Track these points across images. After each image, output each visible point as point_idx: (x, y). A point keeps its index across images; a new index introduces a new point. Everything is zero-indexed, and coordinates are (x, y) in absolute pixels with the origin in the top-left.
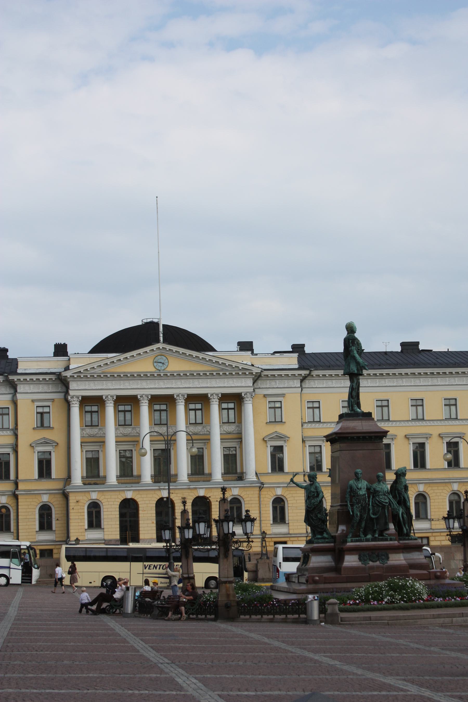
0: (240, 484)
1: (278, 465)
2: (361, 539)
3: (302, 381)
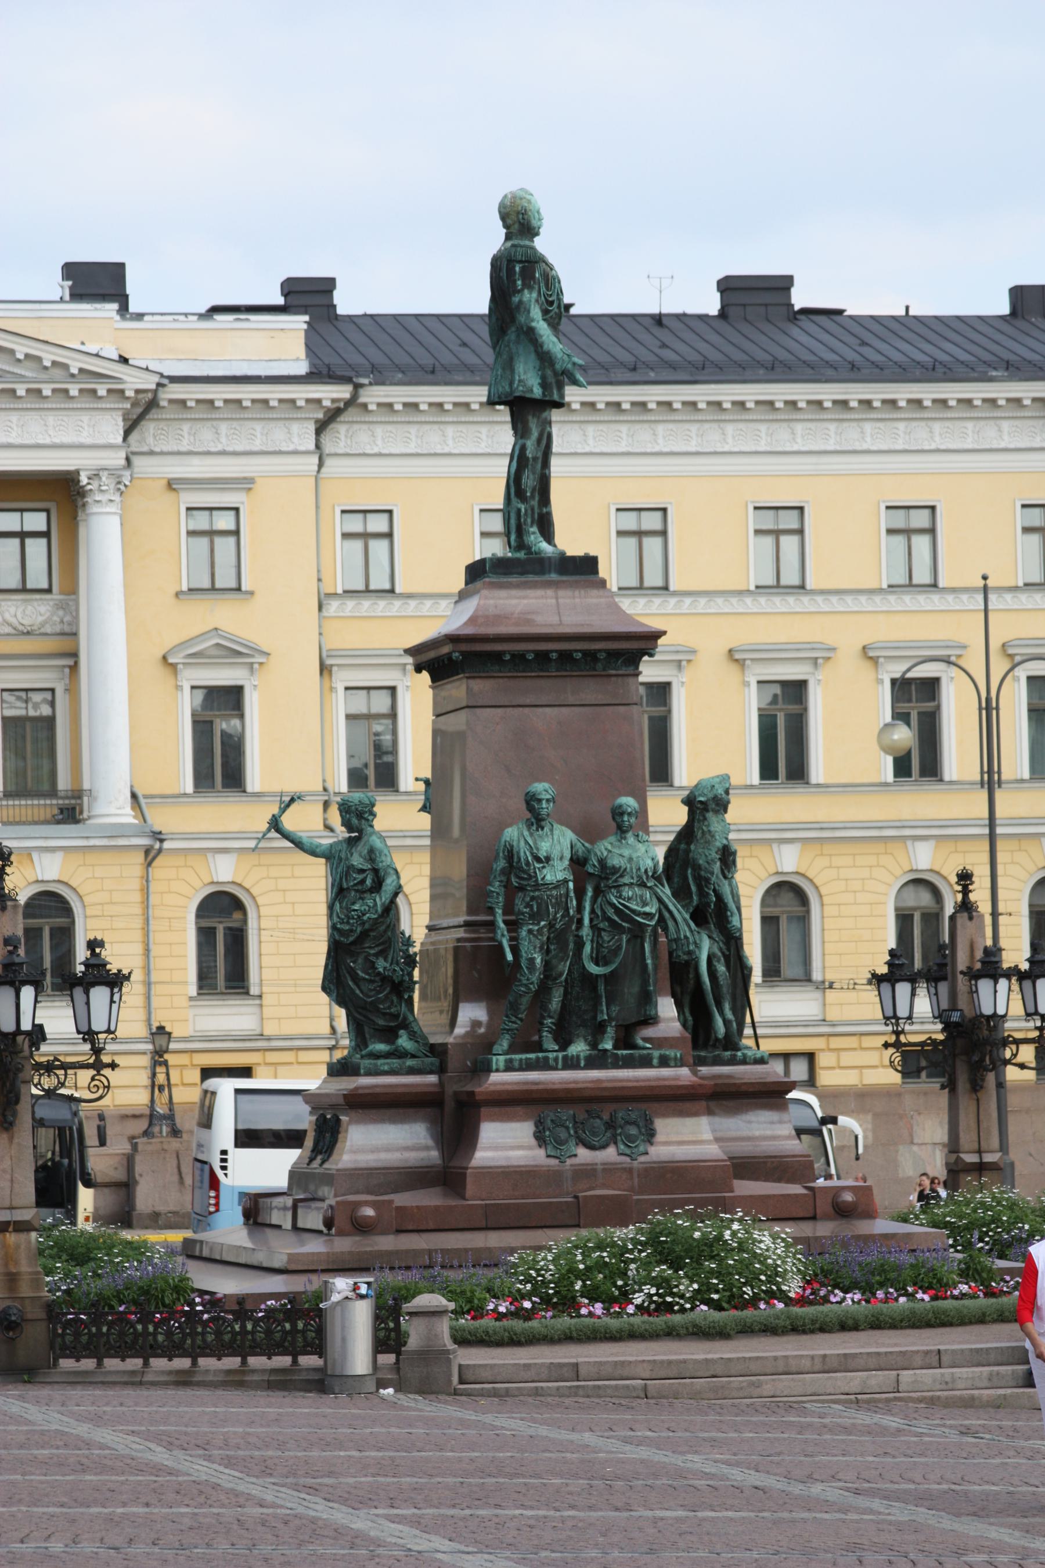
0: (67, 835)
1: (220, 764)
2: (546, 1059)
3: (321, 428)
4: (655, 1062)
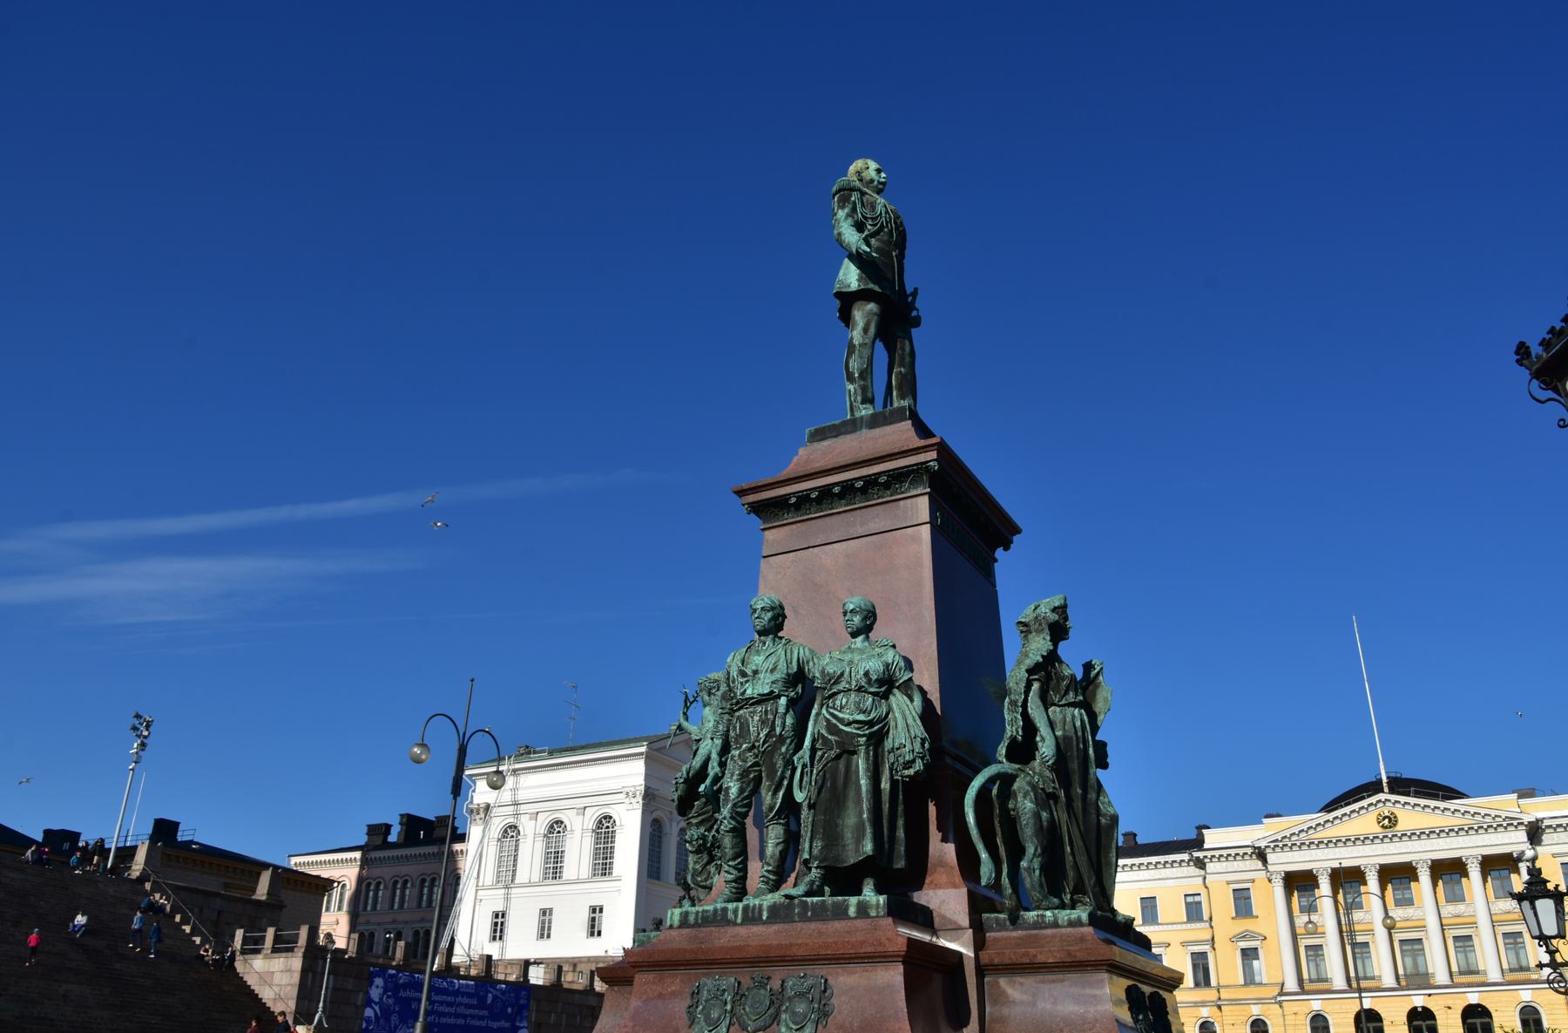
4: (852, 911)
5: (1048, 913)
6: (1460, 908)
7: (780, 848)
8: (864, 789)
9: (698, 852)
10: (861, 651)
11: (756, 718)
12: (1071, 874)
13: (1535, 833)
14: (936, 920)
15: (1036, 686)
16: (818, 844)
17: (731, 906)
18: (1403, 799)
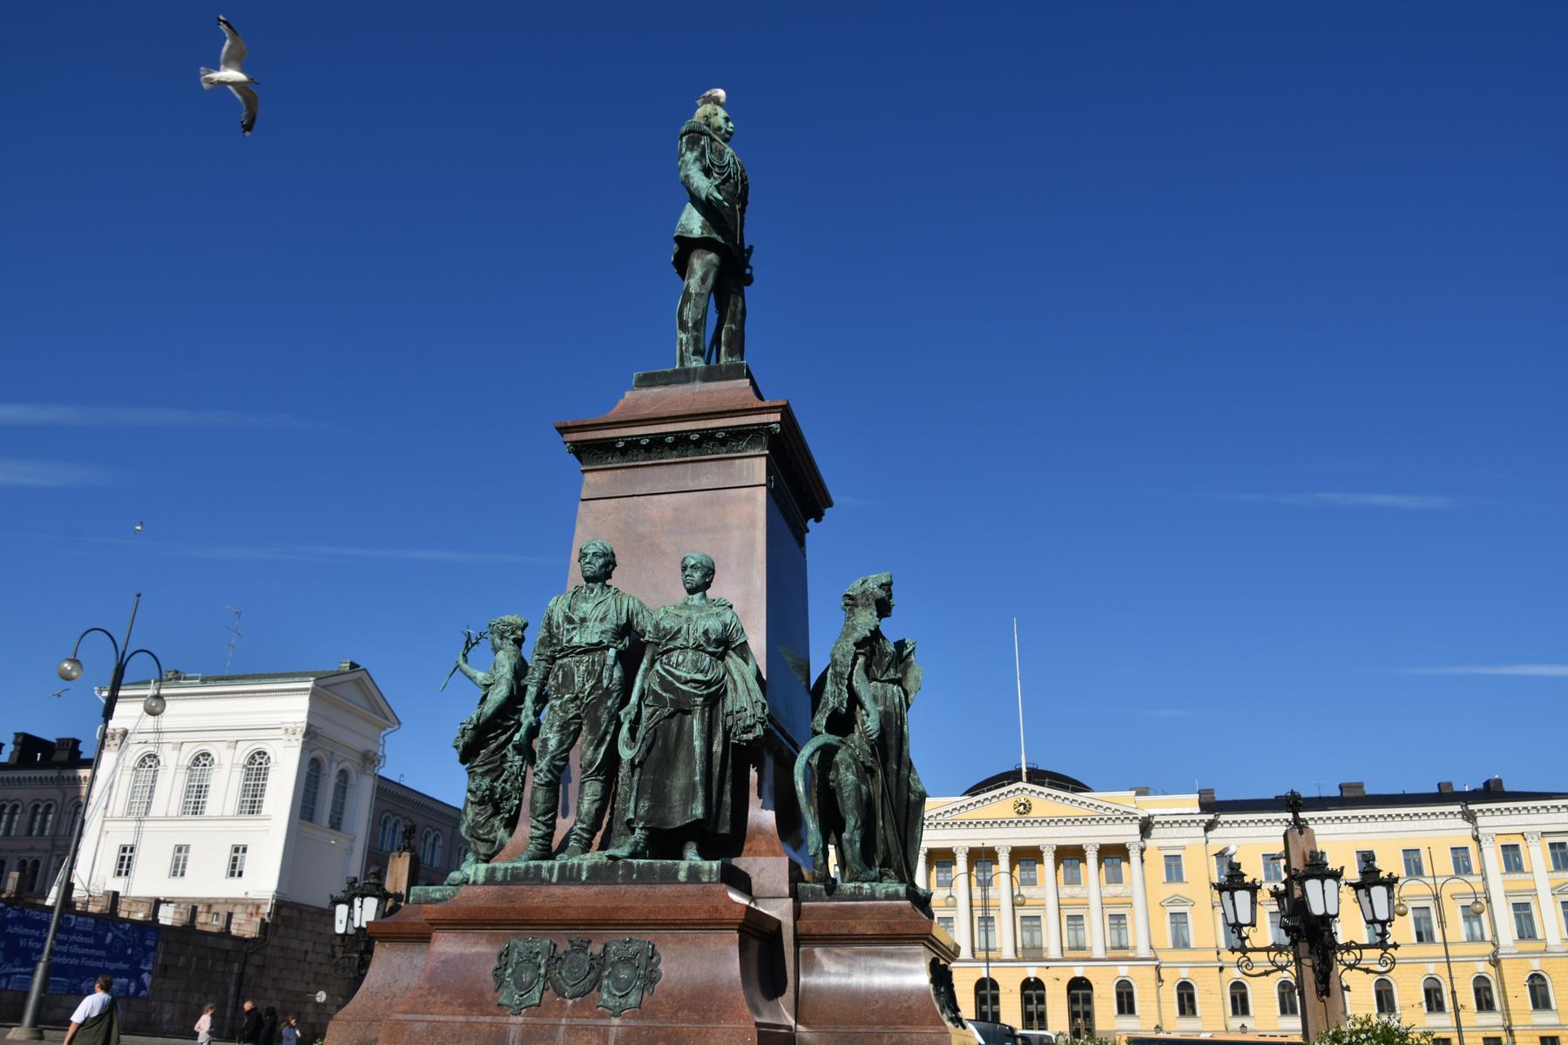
1: (1181, 943)
3: (1207, 829)
4: (682, 876)
5: (866, 886)
6: (1076, 890)
7: (596, 805)
8: (698, 750)
9: (481, 802)
10: (700, 609)
11: (582, 668)
12: (881, 847)
13: (1146, 827)
14: (755, 887)
15: (861, 660)
16: (644, 805)
17: (545, 864)
18: (1038, 788)
